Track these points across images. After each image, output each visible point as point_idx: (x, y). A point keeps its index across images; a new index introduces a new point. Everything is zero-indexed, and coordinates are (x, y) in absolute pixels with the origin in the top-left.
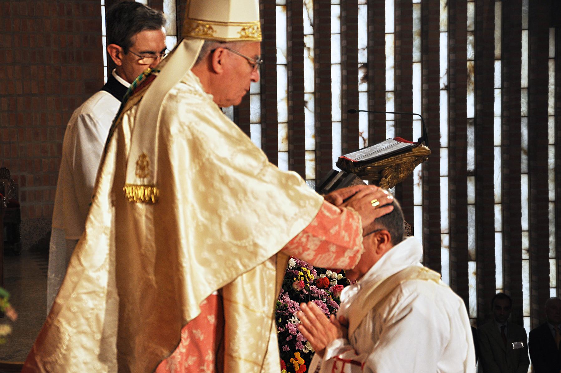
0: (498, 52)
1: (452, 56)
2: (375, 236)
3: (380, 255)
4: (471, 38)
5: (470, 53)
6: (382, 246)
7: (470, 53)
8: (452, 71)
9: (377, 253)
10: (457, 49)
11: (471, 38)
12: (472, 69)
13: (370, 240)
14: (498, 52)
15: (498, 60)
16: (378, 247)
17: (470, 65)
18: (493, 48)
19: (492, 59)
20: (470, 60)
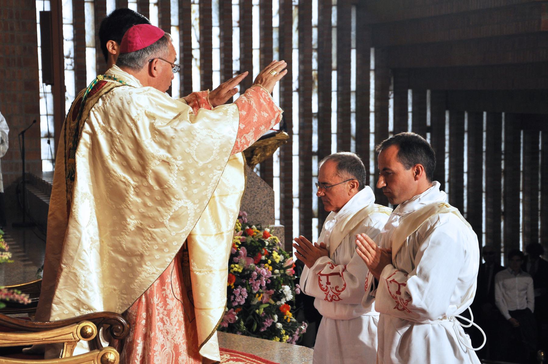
0: (334, 64)
1: (302, 67)
2: (349, 183)
3: (351, 196)
4: (315, 54)
5: (315, 65)
6: (353, 190)
7: (315, 65)
8: (301, 78)
9: (349, 195)
10: (305, 62)
11: (315, 54)
12: (316, 77)
13: (346, 186)
14: (334, 64)
15: (334, 70)
16: (350, 191)
17: (314, 73)
18: (331, 62)
19: (330, 70)
20: (315, 70)
